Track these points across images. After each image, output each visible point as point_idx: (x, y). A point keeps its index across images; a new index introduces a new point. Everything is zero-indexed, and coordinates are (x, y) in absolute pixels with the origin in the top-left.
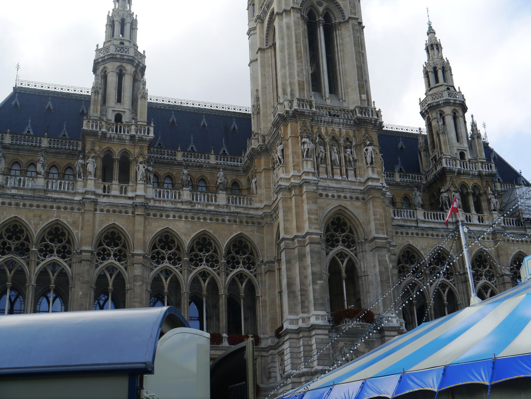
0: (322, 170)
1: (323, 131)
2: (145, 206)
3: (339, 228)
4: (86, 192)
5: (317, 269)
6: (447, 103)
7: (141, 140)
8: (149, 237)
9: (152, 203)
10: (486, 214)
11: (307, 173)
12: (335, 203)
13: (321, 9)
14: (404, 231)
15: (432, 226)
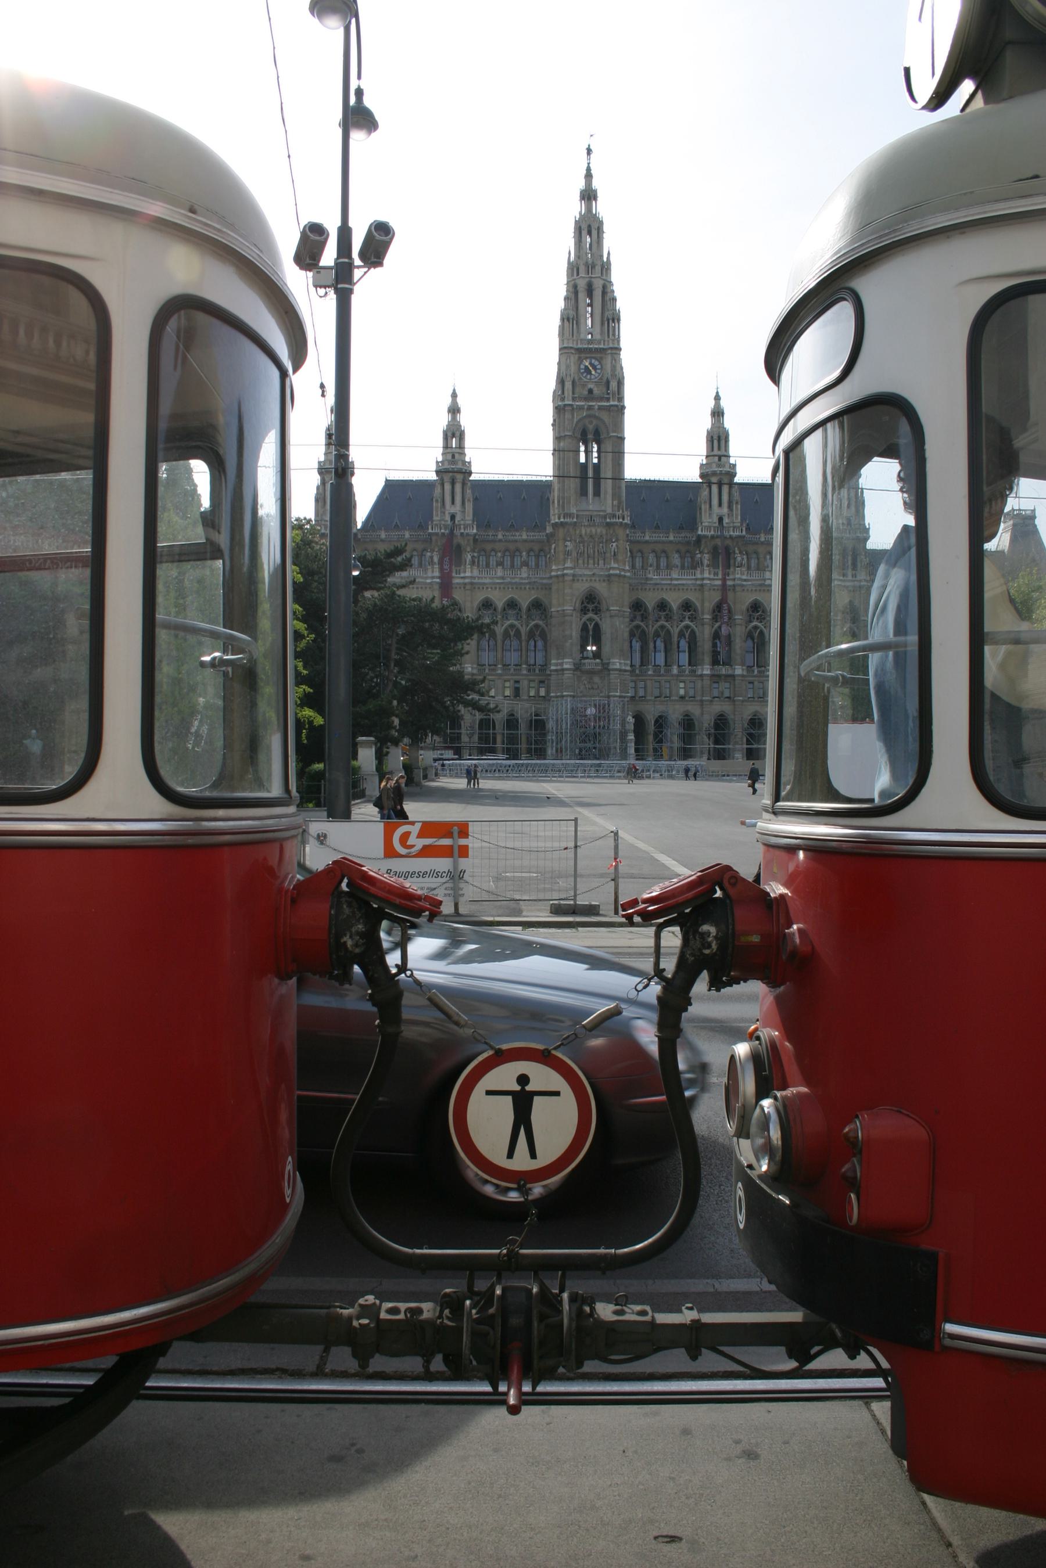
0: (580, 561)
1: (583, 532)
2: (472, 584)
3: (591, 602)
4: (433, 578)
5: (567, 633)
6: (714, 474)
7: (468, 534)
8: (476, 604)
9: (476, 581)
10: (732, 569)
11: (567, 568)
12: (587, 585)
13: (591, 427)
14: (660, 587)
15: (684, 582)
